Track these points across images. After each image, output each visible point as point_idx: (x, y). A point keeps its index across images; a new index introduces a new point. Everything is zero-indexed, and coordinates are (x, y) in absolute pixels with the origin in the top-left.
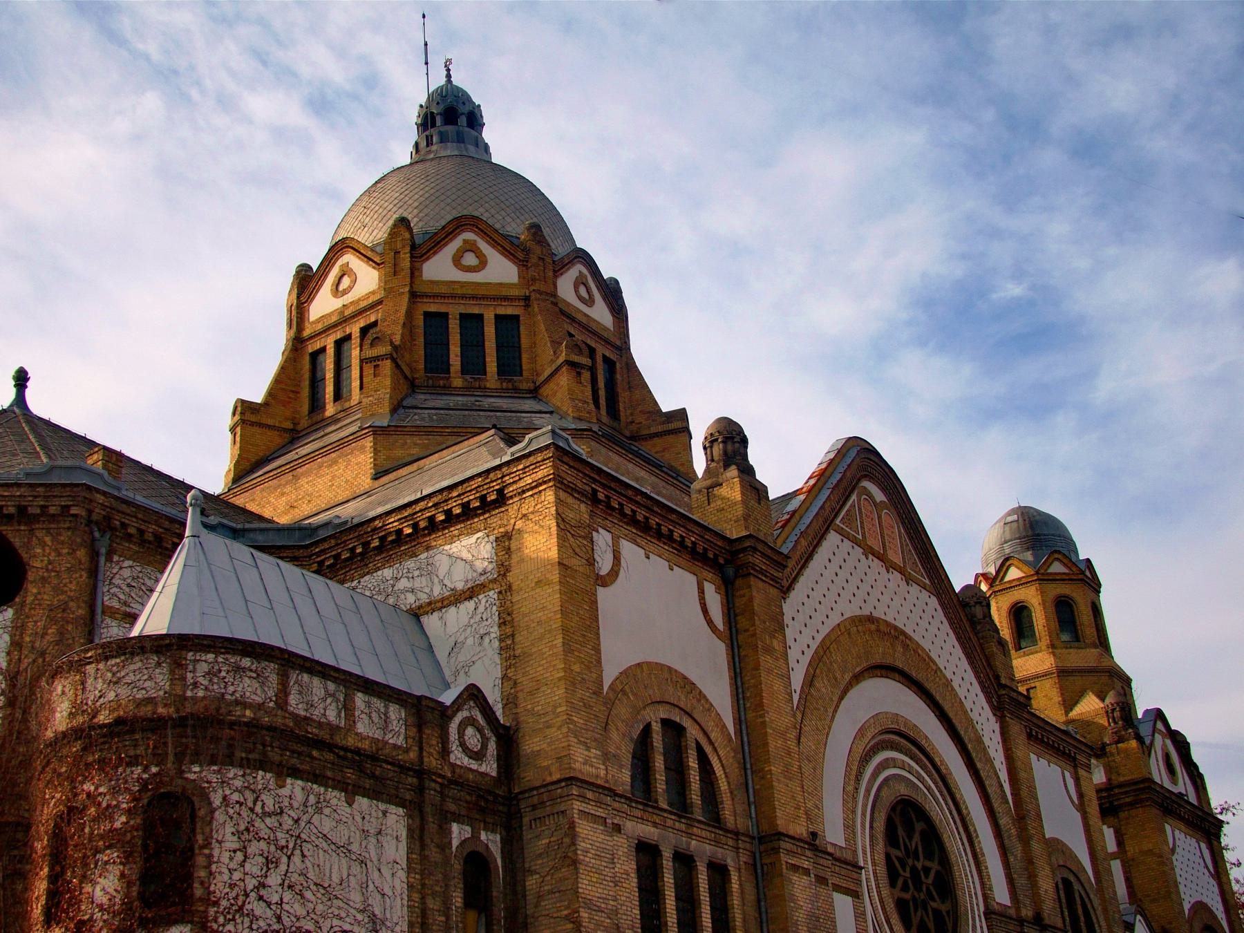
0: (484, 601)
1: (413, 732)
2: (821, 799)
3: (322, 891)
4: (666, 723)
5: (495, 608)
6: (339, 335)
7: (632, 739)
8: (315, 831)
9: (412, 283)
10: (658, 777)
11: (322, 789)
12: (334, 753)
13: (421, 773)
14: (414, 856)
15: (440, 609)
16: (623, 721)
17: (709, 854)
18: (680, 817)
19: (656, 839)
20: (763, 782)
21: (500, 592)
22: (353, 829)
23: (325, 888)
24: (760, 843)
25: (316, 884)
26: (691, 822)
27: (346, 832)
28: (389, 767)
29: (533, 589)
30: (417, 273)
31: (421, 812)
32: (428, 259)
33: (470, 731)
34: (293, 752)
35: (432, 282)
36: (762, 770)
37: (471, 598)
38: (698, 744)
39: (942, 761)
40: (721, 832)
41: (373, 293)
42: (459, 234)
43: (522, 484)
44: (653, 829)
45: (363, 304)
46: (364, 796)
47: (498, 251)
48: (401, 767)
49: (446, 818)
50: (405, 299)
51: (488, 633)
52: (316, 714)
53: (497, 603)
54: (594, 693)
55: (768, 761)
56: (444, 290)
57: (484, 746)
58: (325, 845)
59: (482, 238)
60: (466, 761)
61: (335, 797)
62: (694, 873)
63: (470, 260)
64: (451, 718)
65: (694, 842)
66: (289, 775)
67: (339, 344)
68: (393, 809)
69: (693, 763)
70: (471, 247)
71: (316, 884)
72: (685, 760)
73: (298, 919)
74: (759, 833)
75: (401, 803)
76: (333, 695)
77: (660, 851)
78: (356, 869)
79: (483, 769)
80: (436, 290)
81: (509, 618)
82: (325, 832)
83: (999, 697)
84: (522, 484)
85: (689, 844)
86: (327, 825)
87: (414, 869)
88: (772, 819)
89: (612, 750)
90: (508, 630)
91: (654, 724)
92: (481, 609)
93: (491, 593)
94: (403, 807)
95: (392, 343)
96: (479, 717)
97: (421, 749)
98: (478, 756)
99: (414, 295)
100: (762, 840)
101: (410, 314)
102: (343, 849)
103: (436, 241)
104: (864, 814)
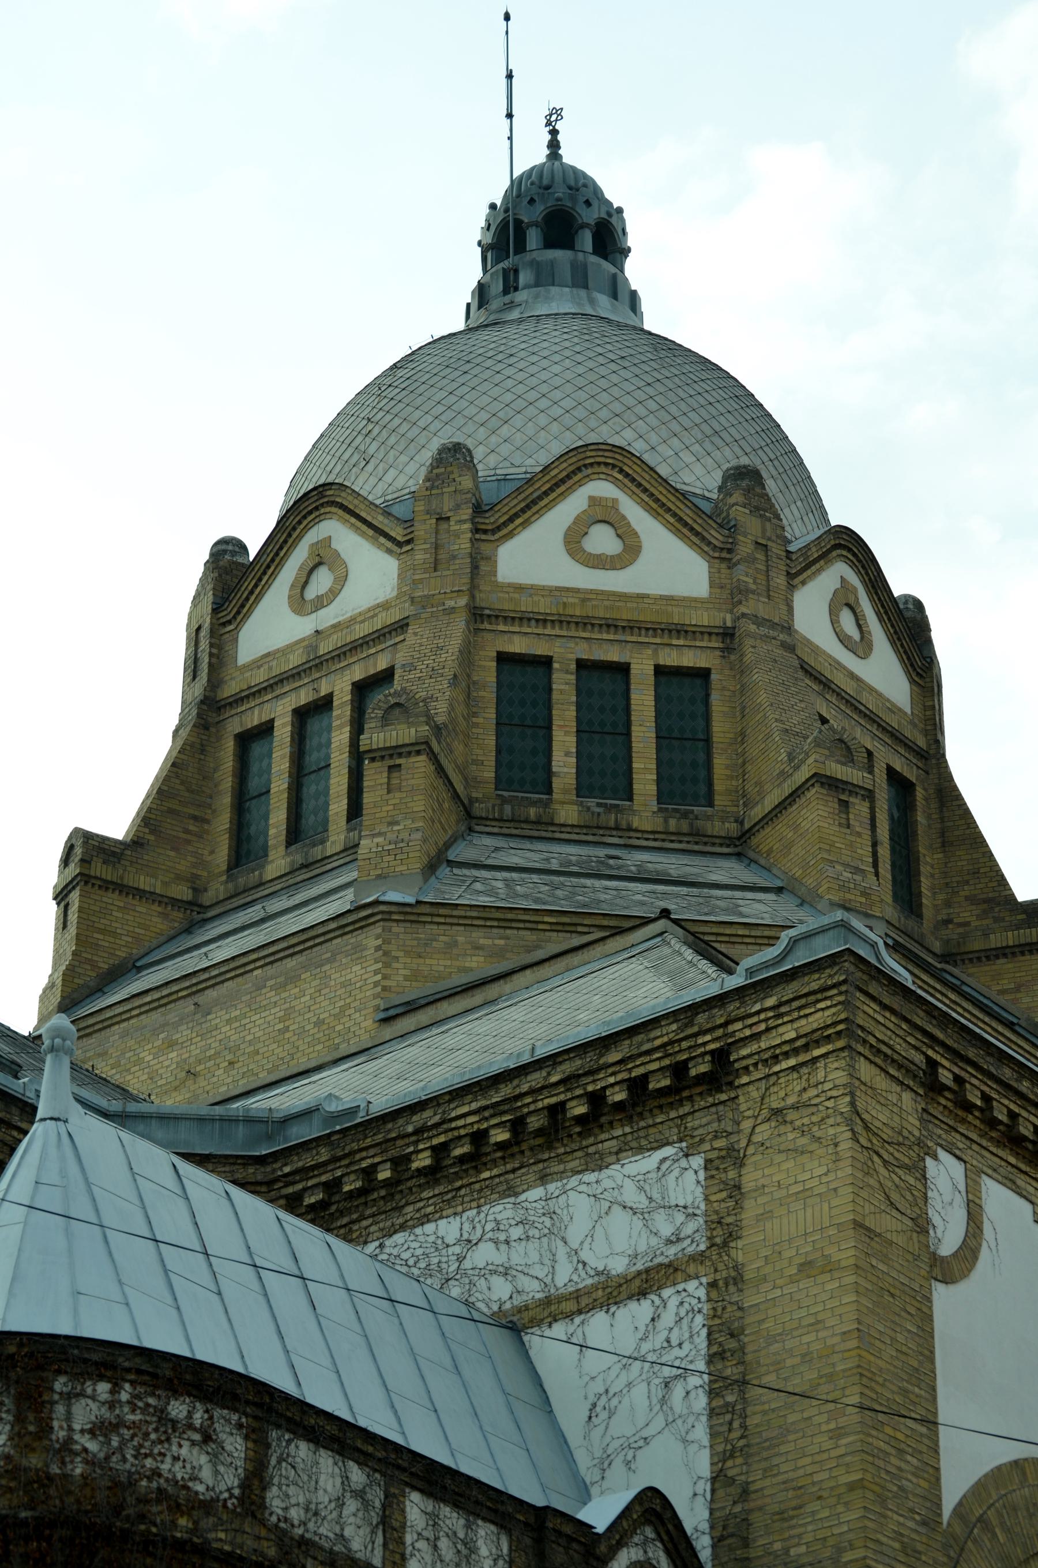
0: (673, 1302)
5: (699, 1320)
15: (570, 1316)
30: (484, 567)
32: (510, 535)
35: (520, 588)
37: (642, 1294)
42: (580, 484)
50: (459, 625)
53: (706, 1308)
56: (543, 606)
80: (526, 605)
81: (732, 1344)
92: (668, 1318)
93: (692, 1286)
95: (429, 719)
101: (467, 656)
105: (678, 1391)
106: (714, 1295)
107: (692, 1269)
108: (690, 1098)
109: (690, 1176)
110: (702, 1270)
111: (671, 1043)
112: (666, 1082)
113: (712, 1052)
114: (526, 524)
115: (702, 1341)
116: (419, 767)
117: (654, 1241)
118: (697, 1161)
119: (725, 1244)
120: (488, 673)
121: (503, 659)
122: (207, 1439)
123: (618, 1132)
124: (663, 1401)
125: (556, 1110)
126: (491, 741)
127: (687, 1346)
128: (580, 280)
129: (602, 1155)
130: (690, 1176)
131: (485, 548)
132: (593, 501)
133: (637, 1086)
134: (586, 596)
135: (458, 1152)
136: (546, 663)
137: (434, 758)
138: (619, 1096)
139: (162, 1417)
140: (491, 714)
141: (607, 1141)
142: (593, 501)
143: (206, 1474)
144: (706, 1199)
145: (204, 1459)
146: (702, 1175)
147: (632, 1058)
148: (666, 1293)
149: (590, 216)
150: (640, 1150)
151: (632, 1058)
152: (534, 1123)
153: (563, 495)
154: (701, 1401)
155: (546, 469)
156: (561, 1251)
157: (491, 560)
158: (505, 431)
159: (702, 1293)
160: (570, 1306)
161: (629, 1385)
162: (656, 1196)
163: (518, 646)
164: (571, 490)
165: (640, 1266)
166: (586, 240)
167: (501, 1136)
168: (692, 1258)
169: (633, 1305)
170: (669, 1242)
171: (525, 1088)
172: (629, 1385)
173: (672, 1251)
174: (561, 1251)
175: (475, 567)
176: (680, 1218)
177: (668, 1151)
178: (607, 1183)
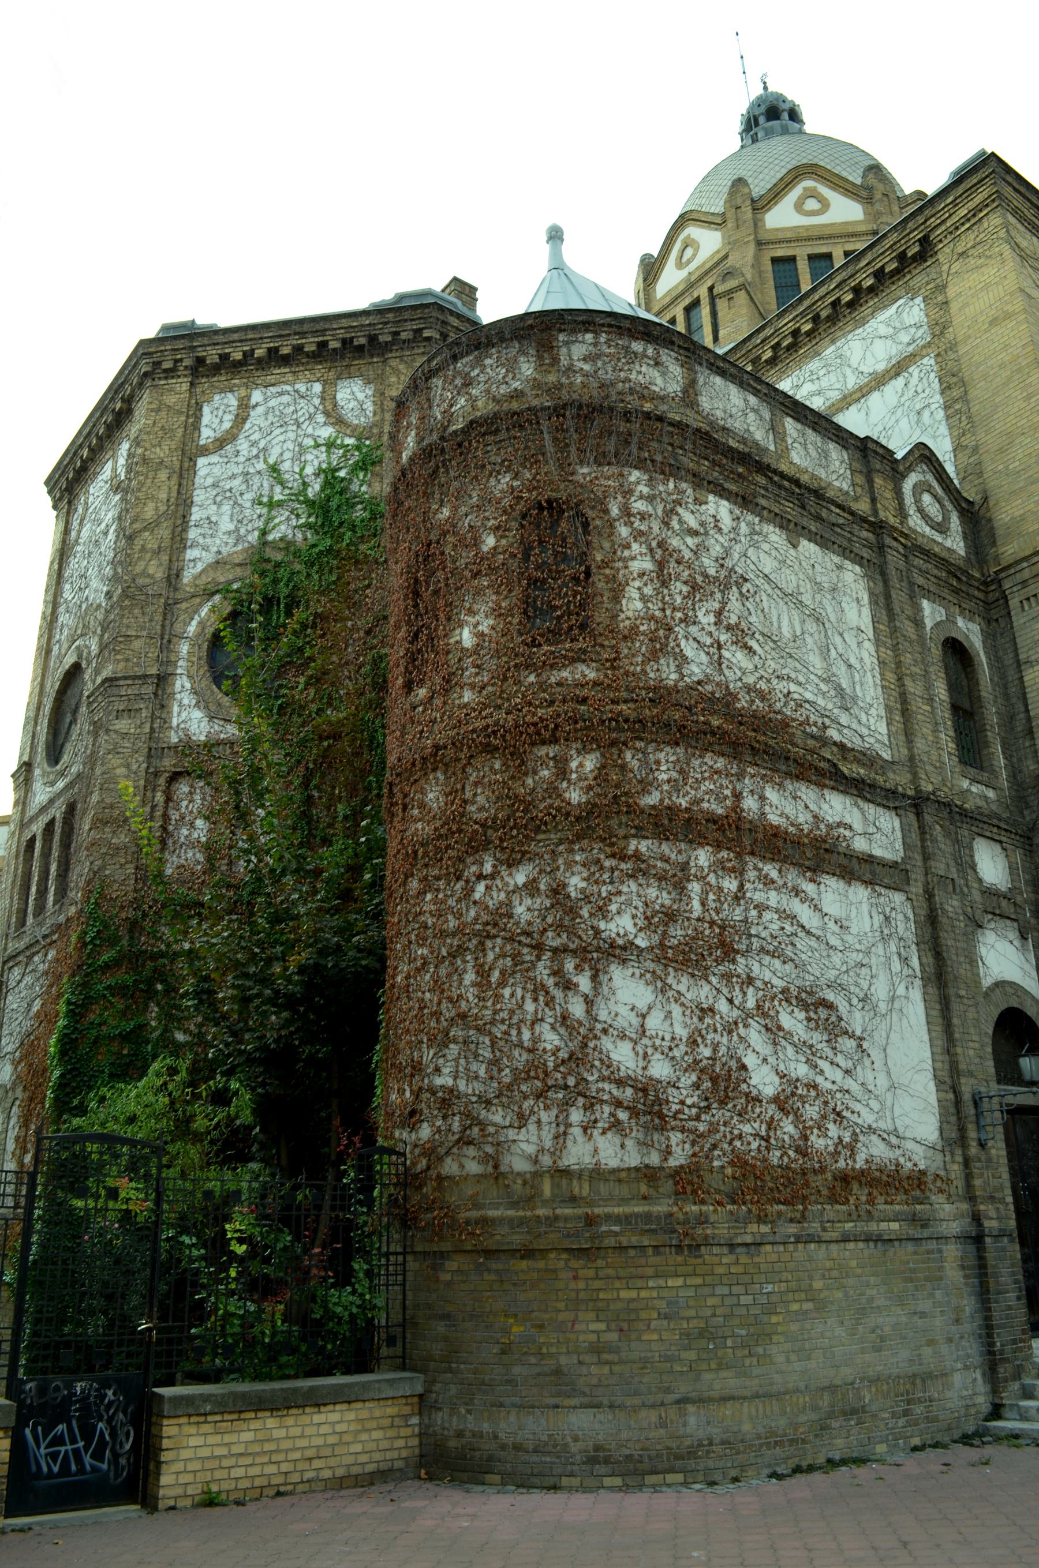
0: (916, 373)
1: (860, 479)
3: (772, 644)
5: (933, 375)
6: (687, 301)
8: (752, 567)
9: (756, 233)
11: (757, 520)
12: (766, 476)
13: (878, 527)
14: (881, 627)
21: (938, 355)
22: (801, 577)
23: (775, 642)
25: (763, 634)
27: (793, 577)
28: (838, 511)
29: (986, 331)
30: (760, 224)
31: (883, 574)
32: (769, 209)
33: (927, 498)
34: (714, 463)
35: (777, 230)
37: (898, 374)
41: (718, 252)
43: (955, 218)
45: (708, 266)
46: (810, 540)
47: (840, 193)
48: (852, 513)
49: (914, 593)
50: (751, 249)
51: (928, 406)
52: (738, 425)
56: (789, 235)
57: (946, 518)
58: (767, 586)
59: (822, 184)
60: (927, 530)
61: (775, 536)
63: (812, 204)
64: (904, 476)
66: (712, 492)
67: (688, 310)
68: (848, 564)
70: (811, 194)
71: (763, 634)
73: (744, 673)
75: (858, 560)
76: (756, 411)
78: (811, 626)
79: (948, 543)
80: (781, 236)
81: (955, 379)
82: (767, 571)
84: (955, 218)
86: (768, 565)
87: (885, 643)
90: (956, 393)
92: (914, 380)
93: (925, 361)
94: (861, 566)
96: (935, 484)
97: (874, 500)
98: (942, 528)
99: (760, 244)
101: (757, 258)
102: (792, 598)
103: (776, 193)
105: (926, 414)
106: (939, 359)
107: (924, 352)
108: (910, 272)
109: (916, 308)
110: (930, 350)
111: (895, 244)
112: (895, 265)
113: (919, 240)
114: (776, 203)
115: (936, 385)
116: (741, 297)
117: (900, 347)
118: (919, 300)
119: (942, 333)
120: (768, 266)
121: (775, 260)
122: (657, 364)
123: (871, 303)
124: (918, 422)
125: (835, 304)
126: (773, 293)
127: (927, 391)
128: (785, 131)
129: (863, 318)
130: (916, 308)
131: (759, 216)
132: (805, 189)
133: (880, 275)
134: (807, 228)
135: (785, 344)
136: (792, 259)
137: (748, 292)
138: (870, 282)
139: (627, 349)
140: (771, 283)
141: (865, 310)
142: (805, 189)
143: (659, 381)
144: (927, 315)
145: (657, 374)
146: (922, 306)
147: (874, 260)
148: (910, 370)
149: (786, 106)
150: (885, 307)
151: (874, 260)
152: (824, 314)
153: (791, 189)
154: (941, 414)
155: (782, 179)
156: (848, 372)
157: (763, 220)
158: (761, 176)
159: (932, 362)
160: (855, 396)
161: (897, 421)
162: (898, 325)
163: (780, 253)
164: (794, 186)
165: (894, 362)
166: (785, 116)
167: (807, 327)
168: (924, 347)
169: (893, 382)
170: (909, 344)
171: (817, 297)
172: (897, 421)
173: (911, 349)
174: (848, 372)
175: (755, 225)
176: (913, 330)
177: (901, 302)
178: (869, 330)
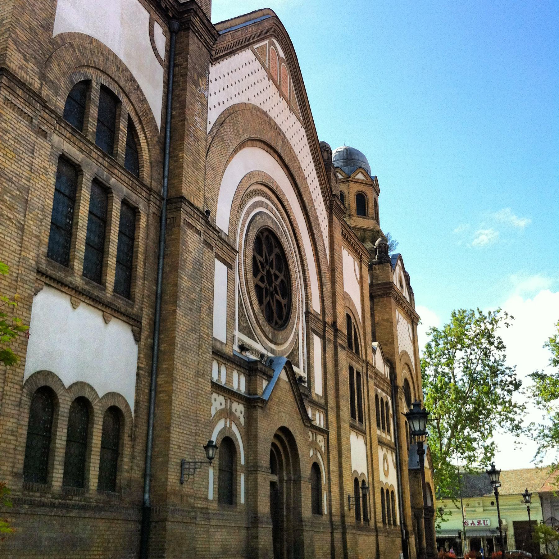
2: (217, 197)
4: (104, 89)
7: (72, 82)
10: (90, 119)
16: (65, 63)
17: (125, 193)
18: (105, 155)
19: (79, 160)
20: (176, 164)
24: (167, 204)
26: (113, 164)
36: (178, 155)
38: (129, 117)
39: (295, 219)
40: (137, 183)
44: (78, 152)
54: (42, 26)
55: (182, 150)
62: (110, 201)
65: (113, 180)
69: (123, 126)
72: (117, 124)
74: (167, 196)
77: (82, 171)
83: (330, 201)
85: (109, 179)
88: (179, 190)
89: (51, 77)
91: (94, 84)
100: (169, 201)
104: (243, 224)
